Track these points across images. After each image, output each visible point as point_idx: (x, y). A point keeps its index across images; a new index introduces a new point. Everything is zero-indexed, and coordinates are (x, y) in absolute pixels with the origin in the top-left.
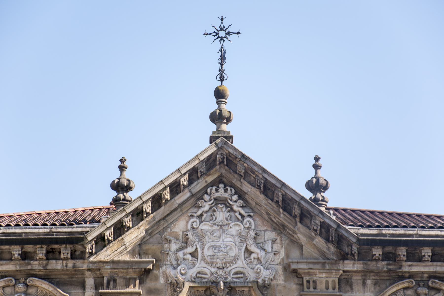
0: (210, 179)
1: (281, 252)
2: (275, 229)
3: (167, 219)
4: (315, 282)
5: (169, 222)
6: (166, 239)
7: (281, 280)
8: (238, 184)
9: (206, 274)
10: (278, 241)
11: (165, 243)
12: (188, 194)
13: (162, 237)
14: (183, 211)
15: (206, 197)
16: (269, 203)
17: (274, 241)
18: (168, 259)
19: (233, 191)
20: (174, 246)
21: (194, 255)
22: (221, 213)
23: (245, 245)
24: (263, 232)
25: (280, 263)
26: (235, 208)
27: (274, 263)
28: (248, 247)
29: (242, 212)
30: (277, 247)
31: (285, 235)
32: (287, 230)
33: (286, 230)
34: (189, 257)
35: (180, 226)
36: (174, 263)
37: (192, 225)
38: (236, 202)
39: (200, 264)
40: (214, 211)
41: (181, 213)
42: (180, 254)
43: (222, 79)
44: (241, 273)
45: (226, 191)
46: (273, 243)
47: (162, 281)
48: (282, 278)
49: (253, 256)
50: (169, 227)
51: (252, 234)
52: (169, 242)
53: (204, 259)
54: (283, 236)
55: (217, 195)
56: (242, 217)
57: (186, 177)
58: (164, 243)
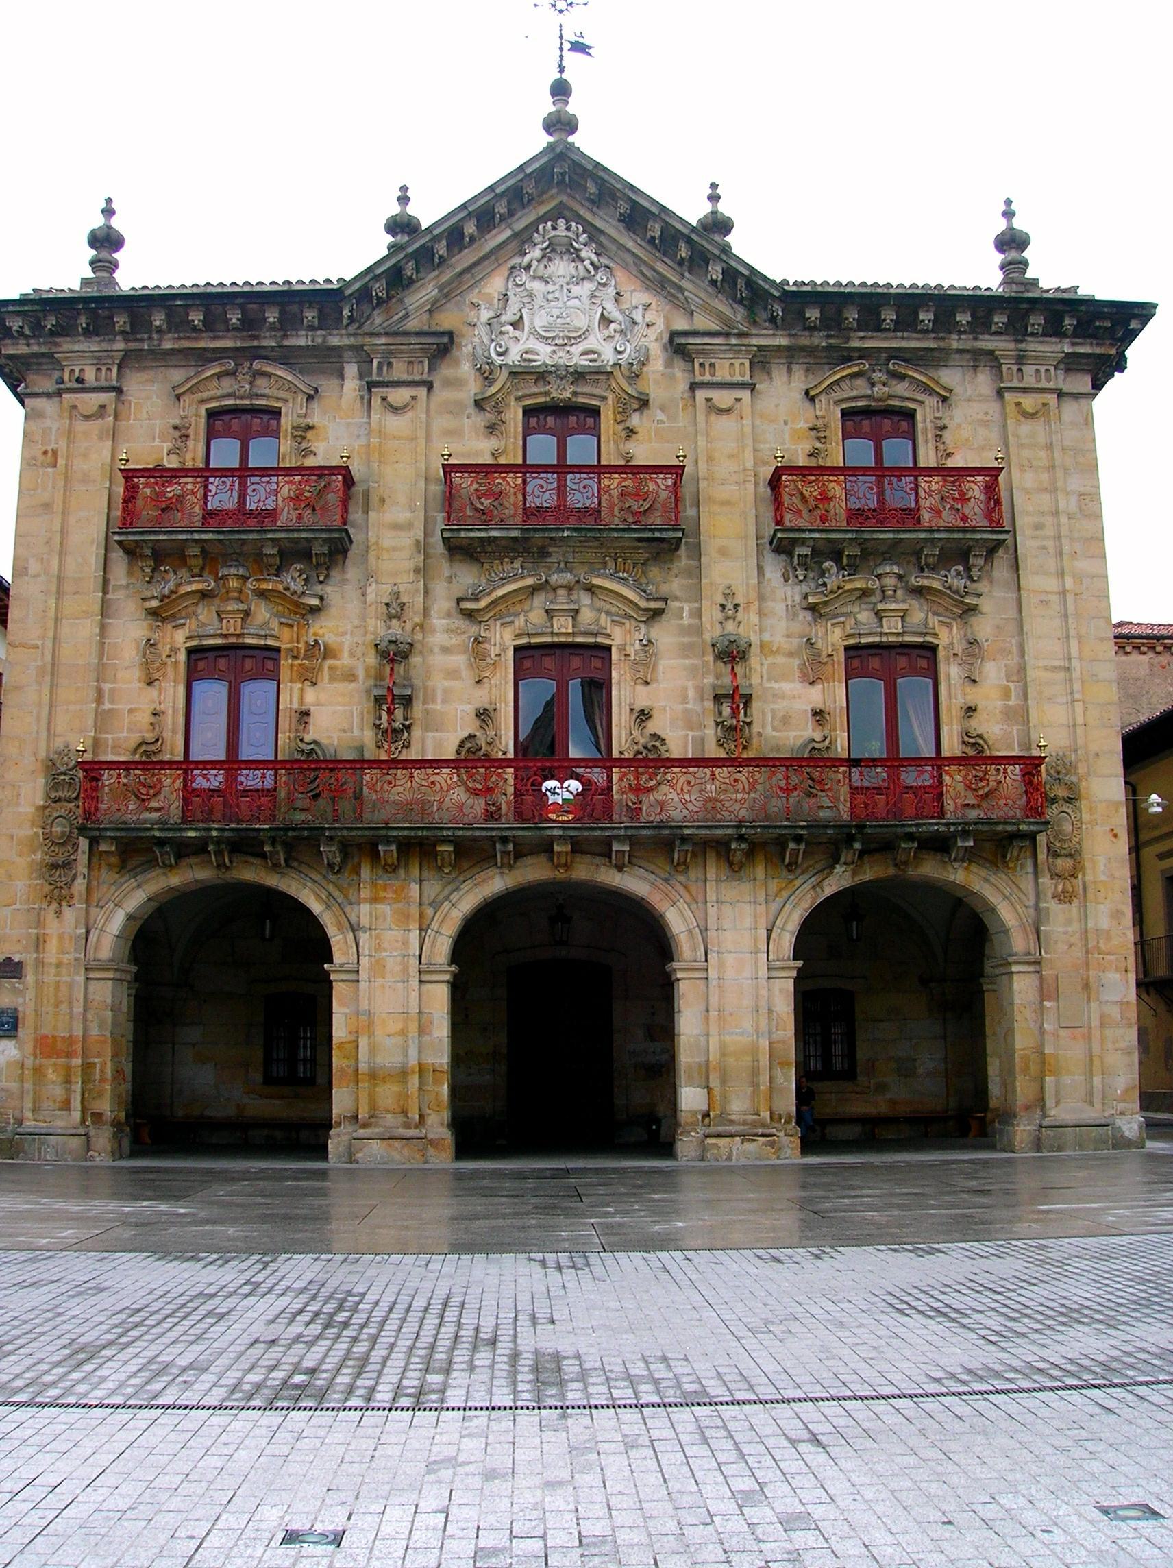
0: (543, 210)
2: (648, 288)
4: (712, 365)
7: (657, 364)
8: (589, 216)
12: (508, 233)
17: (647, 307)
19: (581, 229)
21: (517, 324)
26: (584, 254)
29: (595, 259)
35: (496, 284)
40: (550, 260)
43: (562, 70)
44: (594, 352)
45: (568, 229)
47: (466, 368)
49: (612, 326)
51: (611, 291)
52: (476, 306)
54: (662, 299)
57: (504, 202)
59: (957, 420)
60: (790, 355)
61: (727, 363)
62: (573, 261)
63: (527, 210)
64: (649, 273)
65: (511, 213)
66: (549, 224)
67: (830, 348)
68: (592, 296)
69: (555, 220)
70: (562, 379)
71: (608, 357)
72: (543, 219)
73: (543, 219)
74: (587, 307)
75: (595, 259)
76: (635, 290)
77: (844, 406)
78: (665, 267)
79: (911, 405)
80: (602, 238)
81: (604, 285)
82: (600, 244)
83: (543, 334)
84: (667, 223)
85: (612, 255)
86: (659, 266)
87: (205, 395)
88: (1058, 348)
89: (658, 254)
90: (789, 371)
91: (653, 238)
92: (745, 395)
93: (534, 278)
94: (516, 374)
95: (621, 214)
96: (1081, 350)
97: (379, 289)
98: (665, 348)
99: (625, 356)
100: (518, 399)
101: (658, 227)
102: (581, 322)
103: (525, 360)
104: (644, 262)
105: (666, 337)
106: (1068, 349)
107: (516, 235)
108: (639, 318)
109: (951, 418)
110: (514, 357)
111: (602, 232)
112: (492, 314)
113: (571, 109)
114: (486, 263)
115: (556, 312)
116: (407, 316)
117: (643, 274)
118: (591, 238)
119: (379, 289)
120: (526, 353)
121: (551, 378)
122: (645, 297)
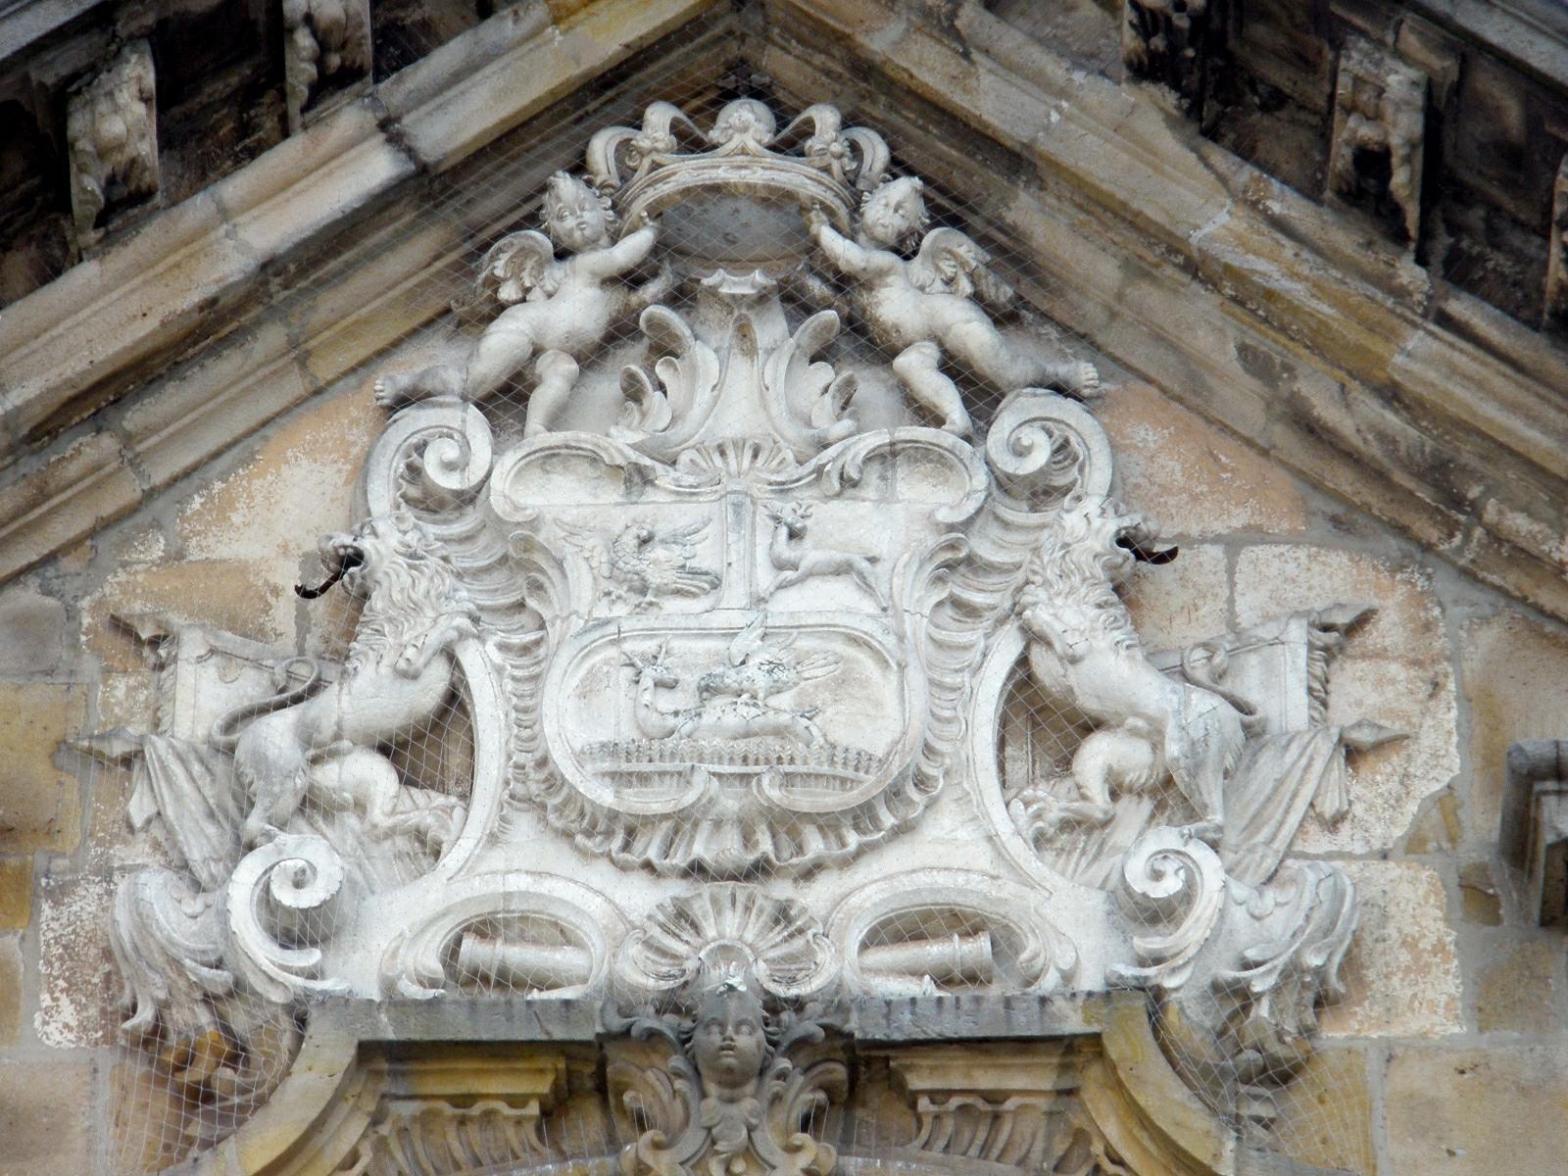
1: (1428, 739)
2: (1344, 524)
3: (134, 418)
5: (160, 475)
6: (122, 627)
8: (928, 65)
9: (565, 936)
10: (1390, 630)
11: (107, 672)
12: (379, 167)
13: (72, 614)
14: (325, 369)
15: (572, 203)
16: (1279, 224)
17: (1340, 636)
18: (139, 808)
19: (877, 152)
20: (202, 693)
22: (740, 366)
23: (1007, 649)
24: (1213, 553)
25: (1414, 845)
26: (896, 304)
27: (1346, 838)
28: (1044, 665)
29: (975, 335)
30: (1364, 693)
31: (1468, 575)
32: (1491, 512)
33: (1476, 510)
34: (376, 775)
35: (281, 507)
36: (200, 843)
37: (414, 472)
38: (904, 248)
39: (493, 839)
40: (665, 348)
41: (295, 385)
42: (277, 732)
44: (961, 922)
46: (1330, 654)
48: (1446, 985)
49: (1097, 755)
50: (157, 525)
51: (1088, 525)
52: (145, 644)
53: (541, 792)
54: (1447, 584)
55: (688, 171)
56: (967, 402)
58: (90, 666)
62: (823, 354)
63: (501, 28)
64: (1355, 417)
65: (398, 43)
66: (660, 117)
68: (955, 562)
69: (702, 104)
70: (733, 1081)
71: (1071, 943)
72: (611, 91)
73: (611, 91)
74: (917, 626)
75: (975, 335)
76: (1255, 535)
78: (1465, 358)
80: (1027, 212)
81: (1041, 492)
82: (1009, 253)
83: (605, 796)
84: (1468, 48)
85: (1093, 313)
86: (1420, 356)
89: (1410, 273)
91: (1373, 161)
93: (549, 459)
94: (391, 1059)
95: (1148, 23)
98: (1475, 897)
99: (1192, 931)
101: (1399, 80)
102: (875, 722)
103: (478, 977)
104: (1320, 342)
105: (1483, 825)
107: (427, 187)
108: (1284, 700)
110: (394, 949)
111: (1018, 162)
112: (251, 687)
114: (227, 366)
115: (692, 656)
117: (1310, 428)
118: (947, 209)
120: (484, 928)
121: (650, 1085)
122: (1334, 577)
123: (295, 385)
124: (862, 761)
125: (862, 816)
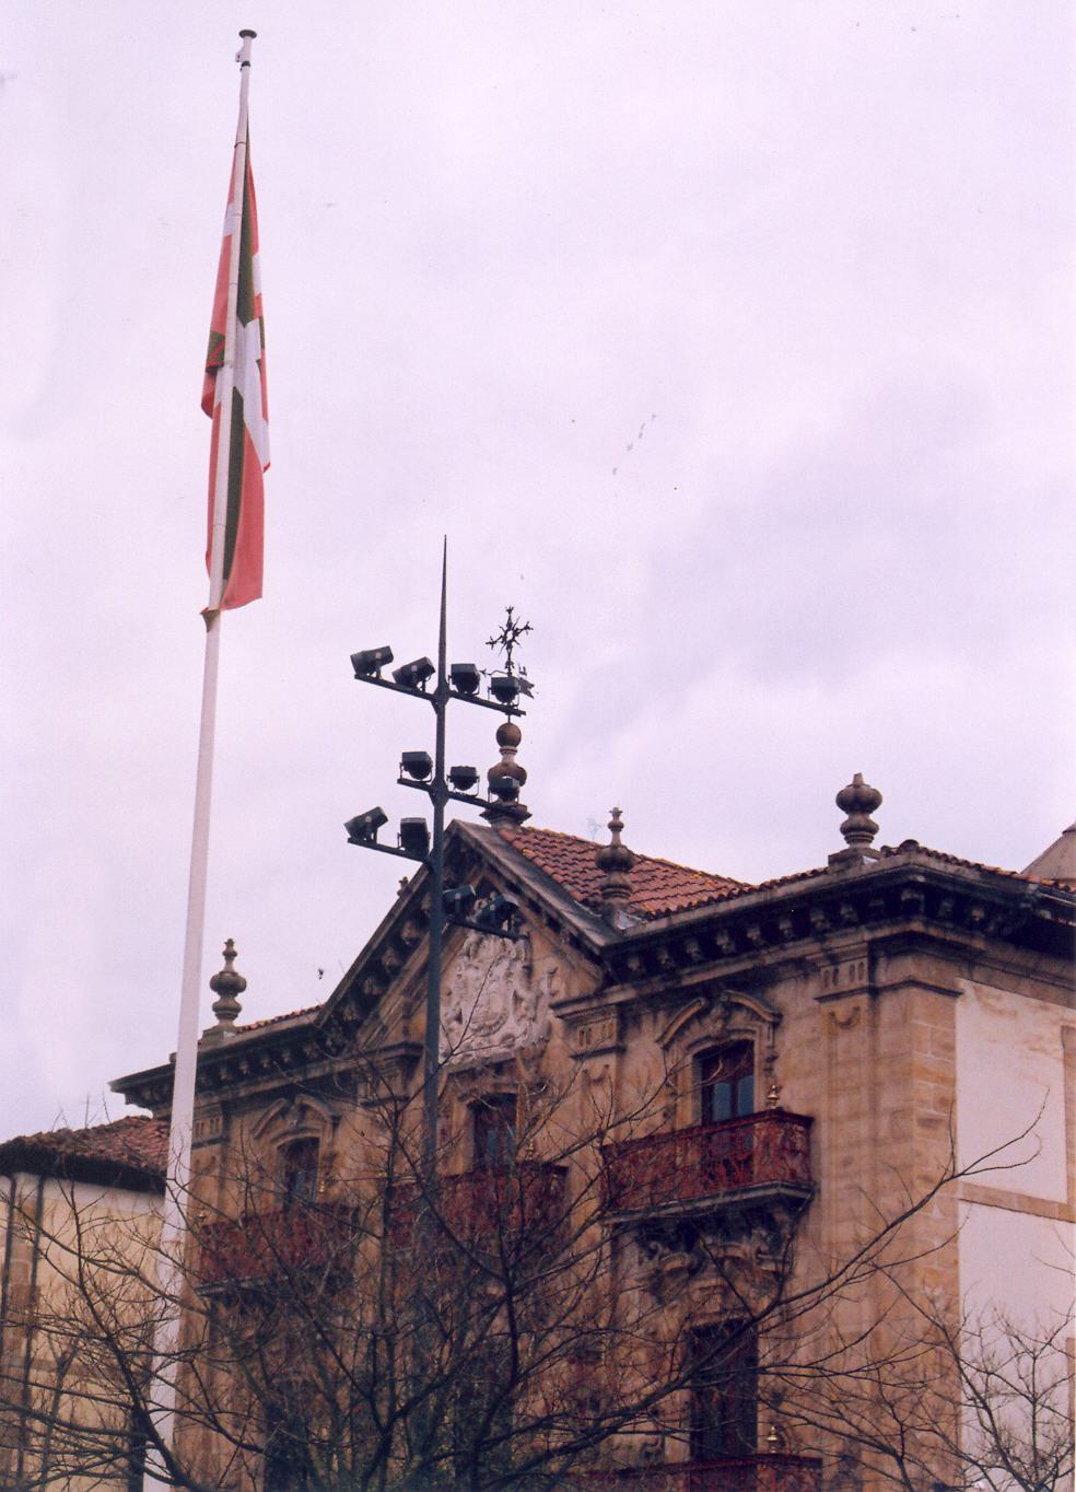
59: (788, 1044)
60: (653, 1002)
61: (600, 1025)
67: (668, 990)
77: (696, 1050)
79: (749, 1037)
87: (273, 1135)
88: (859, 939)
90: (655, 1018)
92: (611, 1060)
96: (880, 934)
97: (350, 1013)
100: (461, 1099)
106: (867, 936)
109: (783, 1043)
113: (519, 759)
116: (385, 1029)
119: (350, 1013)
123: (452, 954)
124: (496, 1014)
125: (497, 1023)
